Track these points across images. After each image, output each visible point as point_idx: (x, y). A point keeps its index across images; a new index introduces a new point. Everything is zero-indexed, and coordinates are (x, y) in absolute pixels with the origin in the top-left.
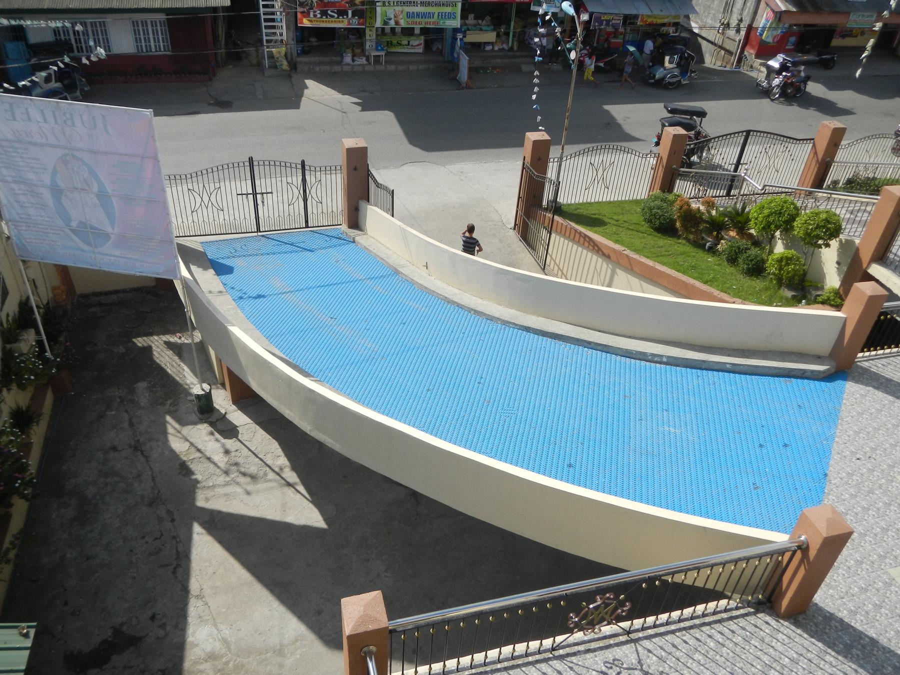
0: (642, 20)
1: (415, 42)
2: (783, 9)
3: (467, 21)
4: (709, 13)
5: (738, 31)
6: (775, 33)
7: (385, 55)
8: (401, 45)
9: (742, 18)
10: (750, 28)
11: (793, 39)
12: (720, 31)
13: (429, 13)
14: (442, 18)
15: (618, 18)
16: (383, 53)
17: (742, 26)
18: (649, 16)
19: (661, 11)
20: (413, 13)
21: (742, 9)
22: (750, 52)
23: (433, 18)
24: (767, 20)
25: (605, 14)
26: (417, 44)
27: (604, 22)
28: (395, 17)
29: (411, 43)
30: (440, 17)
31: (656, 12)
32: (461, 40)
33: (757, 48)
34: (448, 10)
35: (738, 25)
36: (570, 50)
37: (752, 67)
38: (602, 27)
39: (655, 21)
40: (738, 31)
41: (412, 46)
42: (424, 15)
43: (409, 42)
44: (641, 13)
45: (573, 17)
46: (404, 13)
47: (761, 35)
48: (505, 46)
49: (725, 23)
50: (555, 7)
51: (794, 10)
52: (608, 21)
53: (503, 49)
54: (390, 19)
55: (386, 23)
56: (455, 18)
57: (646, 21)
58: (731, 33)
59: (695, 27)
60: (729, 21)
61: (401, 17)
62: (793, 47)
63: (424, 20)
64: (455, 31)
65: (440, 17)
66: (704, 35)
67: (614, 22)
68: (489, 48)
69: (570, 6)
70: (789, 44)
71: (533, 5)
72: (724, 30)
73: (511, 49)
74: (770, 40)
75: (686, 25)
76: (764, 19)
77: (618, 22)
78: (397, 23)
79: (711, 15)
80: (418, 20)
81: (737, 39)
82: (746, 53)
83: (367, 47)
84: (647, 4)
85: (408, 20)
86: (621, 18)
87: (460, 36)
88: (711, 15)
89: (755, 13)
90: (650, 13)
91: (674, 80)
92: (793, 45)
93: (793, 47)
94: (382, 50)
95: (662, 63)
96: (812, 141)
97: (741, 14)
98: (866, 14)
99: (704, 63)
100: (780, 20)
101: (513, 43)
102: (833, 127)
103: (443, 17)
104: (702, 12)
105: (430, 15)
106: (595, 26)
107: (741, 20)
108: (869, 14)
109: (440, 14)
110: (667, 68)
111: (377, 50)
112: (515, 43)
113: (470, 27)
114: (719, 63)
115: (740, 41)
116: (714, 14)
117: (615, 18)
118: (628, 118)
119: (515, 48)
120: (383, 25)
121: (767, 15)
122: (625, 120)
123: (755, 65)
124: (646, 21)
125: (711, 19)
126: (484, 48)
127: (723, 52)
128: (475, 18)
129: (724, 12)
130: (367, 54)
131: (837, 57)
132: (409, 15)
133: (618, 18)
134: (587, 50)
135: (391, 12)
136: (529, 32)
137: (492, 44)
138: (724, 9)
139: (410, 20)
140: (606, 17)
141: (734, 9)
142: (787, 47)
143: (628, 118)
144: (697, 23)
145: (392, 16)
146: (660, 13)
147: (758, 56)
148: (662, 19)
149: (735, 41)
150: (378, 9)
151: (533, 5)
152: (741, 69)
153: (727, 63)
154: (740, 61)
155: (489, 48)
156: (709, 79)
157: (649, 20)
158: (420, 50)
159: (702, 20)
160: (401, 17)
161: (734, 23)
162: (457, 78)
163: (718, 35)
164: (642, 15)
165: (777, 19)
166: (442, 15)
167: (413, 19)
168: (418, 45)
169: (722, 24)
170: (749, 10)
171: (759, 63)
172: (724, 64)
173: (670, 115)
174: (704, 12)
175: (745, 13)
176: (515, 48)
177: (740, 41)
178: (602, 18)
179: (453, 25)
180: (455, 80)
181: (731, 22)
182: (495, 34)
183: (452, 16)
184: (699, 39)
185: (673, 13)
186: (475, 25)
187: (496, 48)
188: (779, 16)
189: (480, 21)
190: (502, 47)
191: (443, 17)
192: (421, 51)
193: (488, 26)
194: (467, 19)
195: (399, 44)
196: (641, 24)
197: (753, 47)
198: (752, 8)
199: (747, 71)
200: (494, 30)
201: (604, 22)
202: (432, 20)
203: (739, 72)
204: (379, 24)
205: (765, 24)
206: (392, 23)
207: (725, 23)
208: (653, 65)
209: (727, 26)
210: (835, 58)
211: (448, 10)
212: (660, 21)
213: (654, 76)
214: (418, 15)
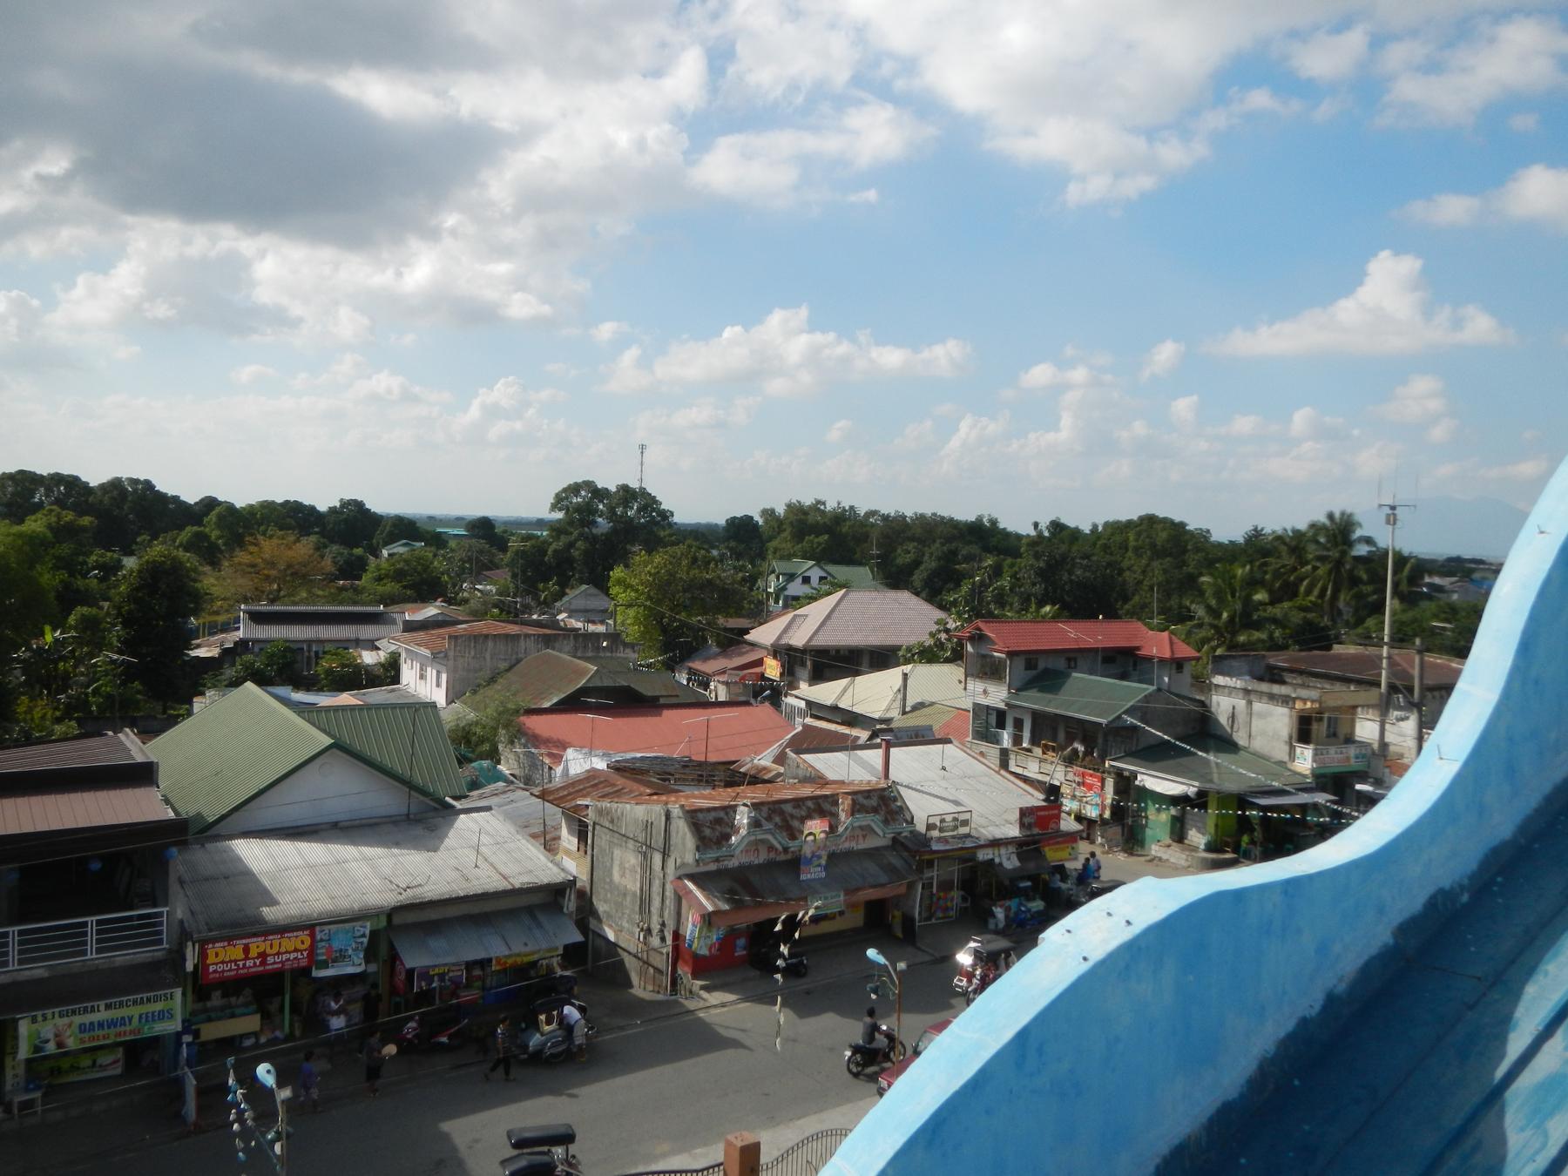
0: (498, 963)
1: (105, 1059)
2: (710, 908)
3: (209, 1004)
4: (623, 914)
5: (663, 939)
6: (709, 942)
7: (45, 1095)
8: (78, 1068)
9: (664, 922)
10: (677, 936)
11: (741, 942)
12: (641, 939)
13: (123, 1018)
14: (147, 1021)
15: (458, 968)
16: (38, 1095)
17: (666, 933)
18: (506, 956)
19: (526, 944)
20: (92, 1024)
21: (662, 909)
22: (684, 971)
23: (130, 1023)
24: (693, 925)
25: (436, 966)
26: (112, 1064)
27: (436, 978)
28: (56, 1036)
29: (98, 1064)
30: (143, 1020)
31: (518, 948)
32: (189, 1044)
33: (691, 963)
34: (158, 1006)
35: (662, 931)
36: (273, 1142)
37: (691, 992)
38: (434, 985)
39: (519, 960)
40: (663, 939)
41: (101, 1066)
42: (112, 1023)
43: (94, 1062)
44: (493, 954)
45: (271, 1090)
46: (75, 1028)
47: (690, 946)
48: (278, 1034)
49: (645, 928)
50: (353, 965)
51: (727, 907)
52: (442, 976)
53: (276, 1038)
54: (47, 1041)
55: (37, 1049)
56: (171, 1017)
57: (506, 963)
58: (655, 941)
59: (611, 936)
60: (649, 925)
61: (68, 1033)
62: (745, 952)
63: (113, 1031)
64: (178, 1035)
65: (143, 1020)
66: (623, 946)
67: (451, 974)
68: (248, 1043)
69: (268, 1072)
70: (738, 949)
71: (316, 969)
72: (645, 938)
73: (290, 1037)
74: (704, 952)
75: (597, 930)
76: (690, 928)
77: (460, 973)
78: (60, 1045)
79: (626, 916)
80: (101, 1033)
81: (664, 951)
82: (680, 972)
83: (8, 1087)
84: (504, 938)
85: (82, 1035)
86: (463, 967)
87: (187, 1038)
88: (626, 916)
89: (679, 914)
90: (507, 953)
91: (561, 1049)
92: (745, 949)
93: (745, 952)
94: (38, 1088)
95: (535, 1026)
96: (722, 1168)
97: (661, 916)
98: (829, 895)
99: (630, 985)
100: (710, 923)
101: (291, 1025)
102: (739, 1144)
103: (150, 1019)
104: (614, 911)
105: (123, 1021)
106: (421, 988)
107: (663, 925)
108: (834, 894)
109: (144, 1016)
110: (546, 1032)
111: (27, 1090)
112: (296, 1025)
113: (213, 1015)
114: (650, 988)
115: (668, 955)
116: (629, 916)
117: (453, 968)
118: (476, 1141)
119: (297, 1033)
120: (34, 1052)
121: (693, 916)
122: (470, 1147)
123: (694, 989)
124: (506, 963)
125: (628, 922)
126: (241, 1042)
127: (651, 970)
128: (224, 996)
129: (641, 913)
130: (7, 1099)
131: (807, 959)
132: (83, 1028)
133: (458, 968)
134: (416, 1021)
135: (47, 1030)
136: (324, 1001)
137: (256, 1034)
138: (640, 908)
139: (86, 1036)
140: (437, 971)
141: (652, 909)
142: (736, 954)
143: (476, 1141)
144: (610, 926)
145: (51, 1036)
146: (524, 950)
147: (695, 976)
148: (529, 955)
149: (662, 953)
150: (24, 1028)
151: (316, 969)
152: (679, 996)
153: (659, 986)
154: (674, 982)
155: (248, 1043)
156: (622, 1028)
157: (510, 961)
158: (117, 1070)
159: (617, 925)
160: (68, 1033)
161: (656, 927)
162: (183, 1112)
163: (640, 946)
164: (497, 958)
165: (707, 922)
166: (147, 1017)
167: (92, 1033)
168: (115, 1062)
169: (642, 930)
170: (670, 908)
171: (698, 987)
172: (656, 989)
173: (515, 1152)
174: (617, 911)
175: (666, 914)
176: (297, 1033)
177: (668, 955)
178: (431, 973)
179: (168, 1028)
180: (178, 1116)
181: (652, 926)
182: (257, 1017)
183: (166, 1014)
184: (619, 950)
185: (544, 946)
186: (222, 1009)
187: (263, 1040)
188: (708, 920)
189: (233, 1000)
190: (273, 1036)
191: (150, 1019)
192: (118, 1071)
193: (246, 1005)
194: (208, 998)
195: (75, 1068)
196: (498, 968)
197: (686, 962)
198: (672, 908)
199: (686, 999)
200: (256, 1012)
201: (436, 978)
202: (128, 1028)
203: (676, 1002)
204: (24, 1052)
205: (692, 932)
206: (51, 1048)
207: (645, 928)
208: (527, 1028)
209: (649, 931)
210: (805, 962)
211: (158, 1006)
212: (526, 959)
213: (527, 1046)
214: (101, 1025)
